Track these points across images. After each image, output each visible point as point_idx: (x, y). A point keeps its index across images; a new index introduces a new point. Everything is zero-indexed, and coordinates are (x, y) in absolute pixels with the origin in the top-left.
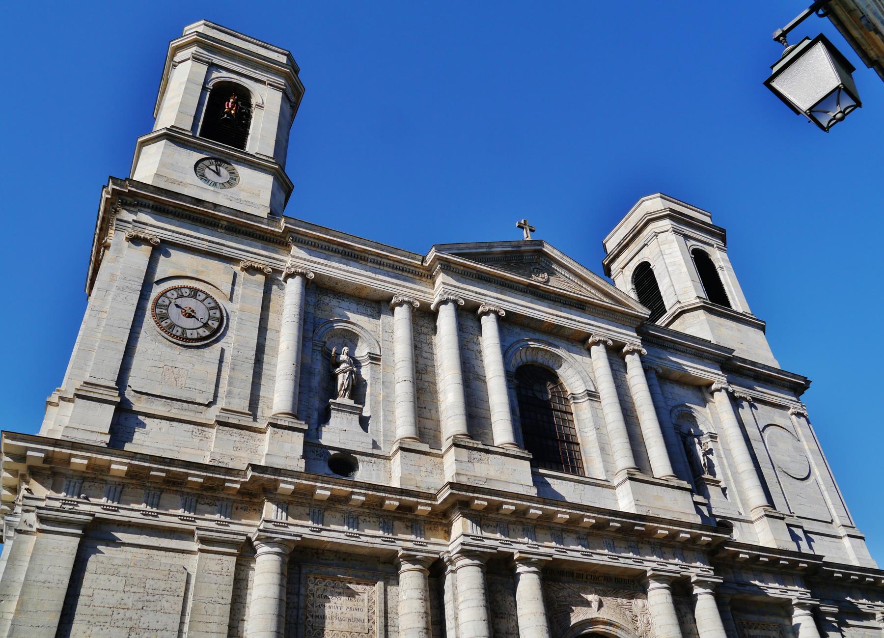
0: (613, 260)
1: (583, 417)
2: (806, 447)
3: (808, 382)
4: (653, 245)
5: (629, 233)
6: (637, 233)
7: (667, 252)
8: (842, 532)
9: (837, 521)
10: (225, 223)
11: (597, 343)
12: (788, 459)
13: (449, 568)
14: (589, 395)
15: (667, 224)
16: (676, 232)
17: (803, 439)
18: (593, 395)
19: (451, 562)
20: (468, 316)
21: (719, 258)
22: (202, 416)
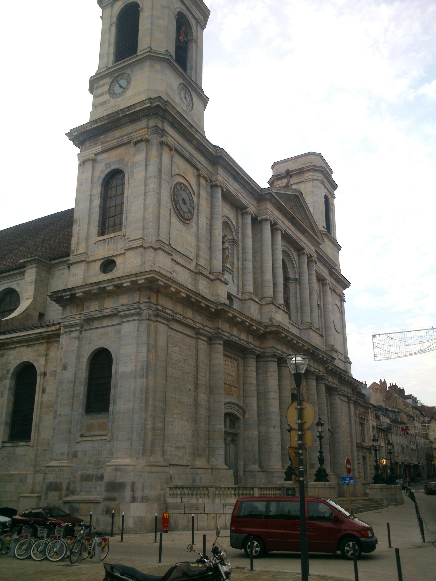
5: (296, 170)
7: (316, 193)
10: (195, 142)
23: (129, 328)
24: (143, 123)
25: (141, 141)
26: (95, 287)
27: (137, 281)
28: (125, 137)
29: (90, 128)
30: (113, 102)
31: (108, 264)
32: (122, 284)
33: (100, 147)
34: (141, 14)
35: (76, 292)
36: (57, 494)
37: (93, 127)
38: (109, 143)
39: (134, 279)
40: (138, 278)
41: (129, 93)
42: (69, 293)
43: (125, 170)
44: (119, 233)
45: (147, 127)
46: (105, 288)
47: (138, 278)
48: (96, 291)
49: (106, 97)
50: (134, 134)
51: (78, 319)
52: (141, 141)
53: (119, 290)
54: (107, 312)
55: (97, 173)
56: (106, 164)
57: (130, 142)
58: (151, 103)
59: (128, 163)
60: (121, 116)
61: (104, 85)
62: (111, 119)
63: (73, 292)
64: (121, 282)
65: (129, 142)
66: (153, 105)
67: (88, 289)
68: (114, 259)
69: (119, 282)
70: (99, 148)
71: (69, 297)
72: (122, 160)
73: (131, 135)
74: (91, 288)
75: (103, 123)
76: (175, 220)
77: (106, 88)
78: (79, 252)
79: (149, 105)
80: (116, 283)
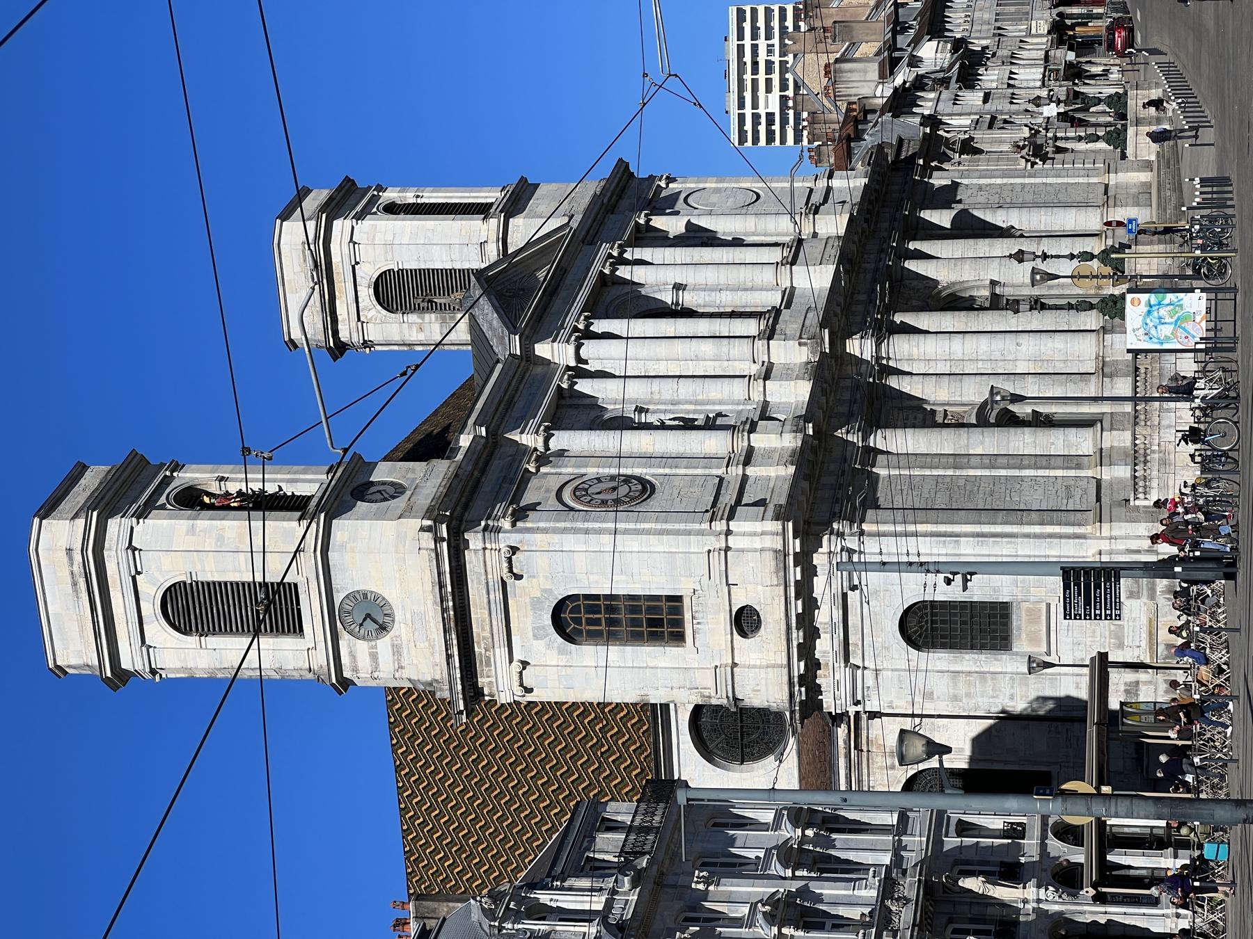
0: (336, 333)
1: (701, 301)
2: (714, 185)
4: (364, 253)
6: (323, 270)
7: (389, 238)
8: (822, 184)
9: (810, 185)
11: (614, 271)
12: (731, 200)
13: (884, 362)
14: (678, 290)
15: (341, 226)
16: (359, 217)
17: (701, 186)
18: (678, 287)
19: (879, 358)
20: (589, 335)
21: (391, 195)
22: (732, 483)
24: (472, 560)
26: (795, 635)
27: (795, 554)
28: (492, 597)
29: (458, 671)
30: (400, 629)
31: (745, 621)
32: (796, 582)
33: (497, 650)
34: (202, 578)
35: (796, 674)
36: (1143, 688)
37: (457, 665)
38: (495, 631)
39: (791, 558)
40: (791, 552)
41: (391, 594)
42: (797, 688)
44: (686, 602)
45: (485, 549)
46: (798, 615)
47: (791, 552)
48: (801, 634)
50: (490, 576)
51: (843, 674)
54: (838, 615)
55: (553, 658)
56: (536, 637)
57: (504, 583)
58: (443, 539)
59: (546, 591)
60: (451, 604)
61: (353, 656)
62: (452, 624)
63: (796, 680)
64: (792, 584)
66: (445, 535)
67: (795, 650)
68: (734, 610)
69: (793, 589)
70: (501, 653)
71: (803, 689)
72: (536, 604)
73: (491, 584)
74: (795, 643)
75: (455, 642)
76: (654, 503)
77: (362, 647)
78: (711, 684)
79: (445, 544)
80: (793, 595)
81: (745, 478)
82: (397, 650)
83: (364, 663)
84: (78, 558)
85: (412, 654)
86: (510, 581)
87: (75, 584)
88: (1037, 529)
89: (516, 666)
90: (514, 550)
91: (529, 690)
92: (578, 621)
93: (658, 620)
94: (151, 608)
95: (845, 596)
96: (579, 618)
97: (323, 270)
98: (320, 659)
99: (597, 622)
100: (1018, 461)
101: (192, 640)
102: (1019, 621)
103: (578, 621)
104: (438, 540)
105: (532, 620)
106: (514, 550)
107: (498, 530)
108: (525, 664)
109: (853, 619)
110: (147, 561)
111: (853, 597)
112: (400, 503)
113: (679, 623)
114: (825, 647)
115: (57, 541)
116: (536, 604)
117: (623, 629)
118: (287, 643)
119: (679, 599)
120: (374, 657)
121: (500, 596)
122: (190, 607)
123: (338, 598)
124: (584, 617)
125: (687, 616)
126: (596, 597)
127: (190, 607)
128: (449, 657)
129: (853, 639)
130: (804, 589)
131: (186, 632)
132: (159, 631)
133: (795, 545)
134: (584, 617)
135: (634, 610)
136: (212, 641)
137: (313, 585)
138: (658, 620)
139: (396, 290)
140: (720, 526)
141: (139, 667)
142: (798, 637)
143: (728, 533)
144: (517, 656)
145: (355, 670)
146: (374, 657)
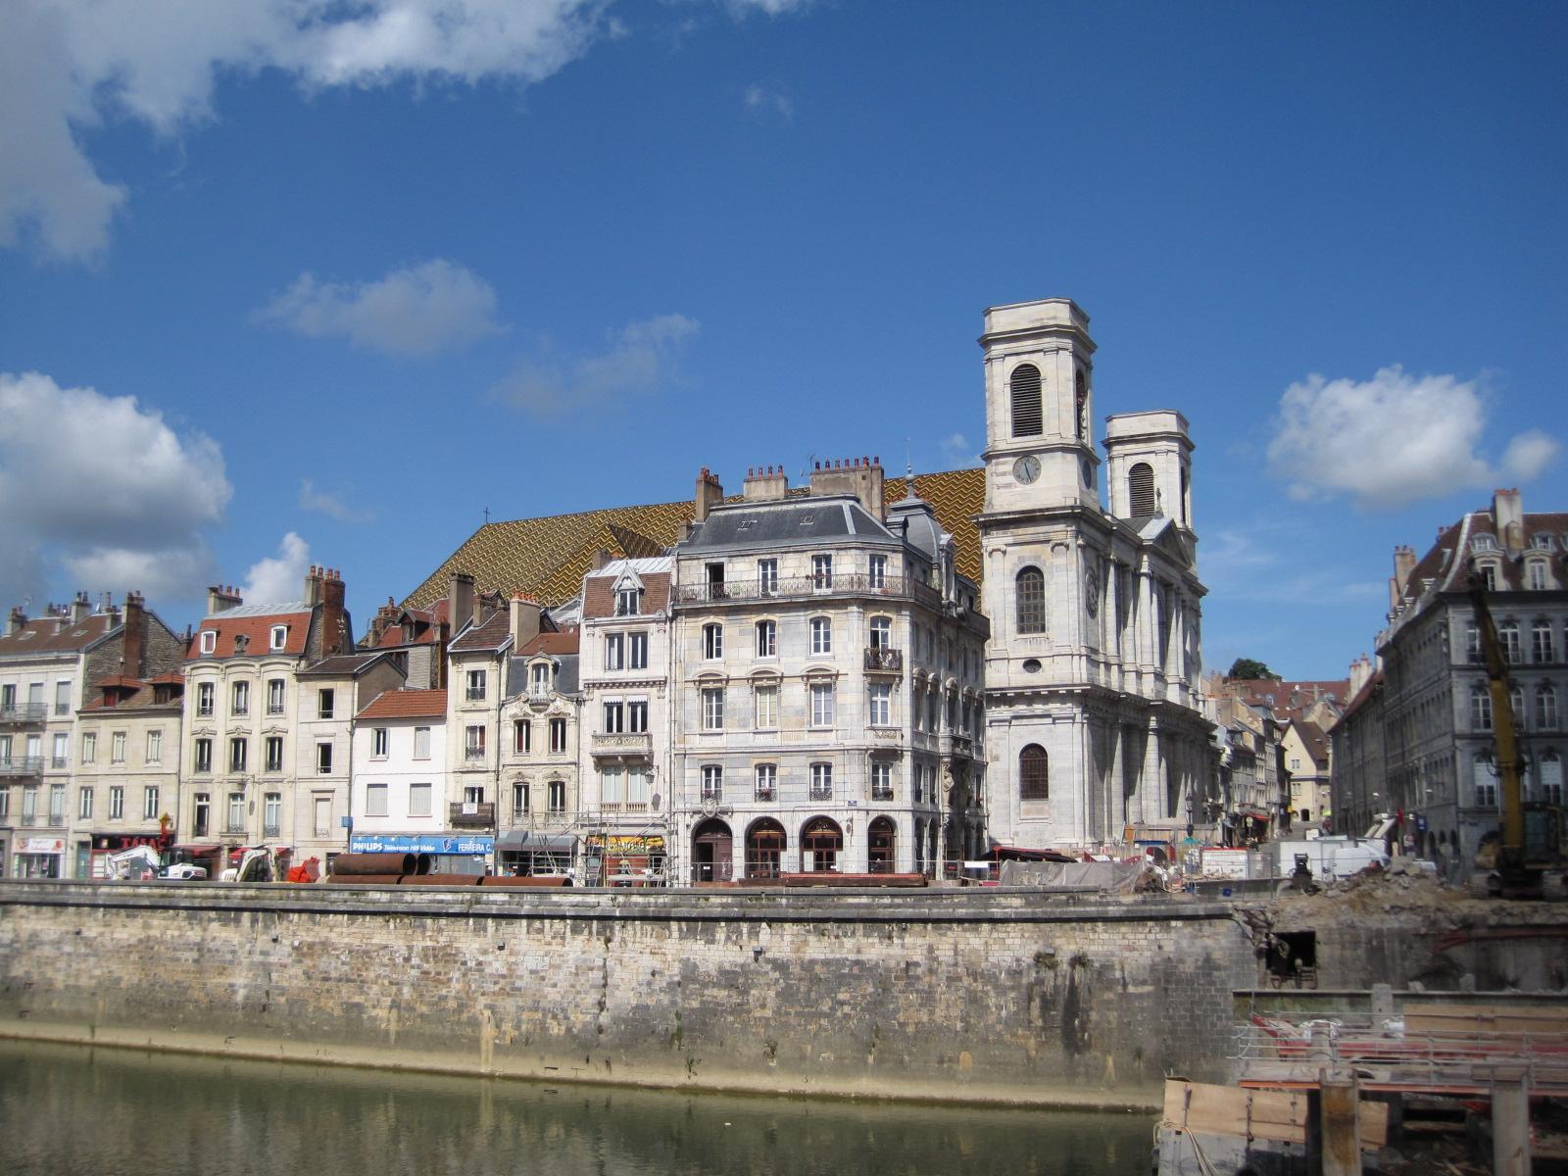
3: (1207, 590)
4: (1162, 457)
23: (1063, 728)
24: (1061, 527)
25: (1061, 544)
30: (1020, 488)
31: (1032, 664)
43: (1045, 570)
44: (1042, 635)
49: (1011, 479)
52: (1061, 544)
53: (1053, 696)
56: (1019, 558)
61: (1005, 463)
65: (1048, 541)
70: (1010, 540)
72: (1037, 558)
77: (1009, 468)
81: (1099, 663)
82: (1008, 486)
83: (1002, 469)
84: (1052, 322)
85: (1005, 494)
86: (1051, 545)
87: (1037, 320)
88: (1087, 812)
89: (1003, 548)
90: (1067, 547)
91: (991, 553)
92: (1028, 579)
93: (1031, 618)
94: (1026, 359)
95: (1049, 716)
96: (1030, 580)
97: (1150, 438)
98: (1002, 446)
99: (1028, 588)
100: (1110, 803)
101: (1008, 380)
102: (1035, 804)
103: (1028, 579)
104: (1072, 507)
105: (1028, 555)
106: (1067, 547)
107: (1077, 538)
108: (1004, 552)
109: (1036, 721)
110: (1052, 357)
111: (1050, 720)
112: (1084, 488)
113: (1029, 631)
114: (1021, 708)
115: (1058, 313)
116: (1037, 558)
117: (1025, 601)
118: (1009, 429)
119: (1043, 629)
120: (1004, 474)
121: (1042, 539)
122: (1026, 382)
123: (1037, 456)
124: (1031, 582)
125: (1035, 635)
126: (1042, 587)
127: (1026, 382)
128: (1009, 513)
129: (1025, 721)
130: (1053, 696)
131: (1012, 377)
132: (1012, 363)
133: (1078, 690)
134: (1031, 582)
135: (1036, 608)
136: (1008, 390)
137: (1042, 443)
138: (1031, 618)
139: (1141, 475)
140: (1083, 651)
141: (993, 353)
142: (1028, 692)
143: (1080, 656)
144: (1009, 549)
145: (997, 464)
146: (1004, 474)
